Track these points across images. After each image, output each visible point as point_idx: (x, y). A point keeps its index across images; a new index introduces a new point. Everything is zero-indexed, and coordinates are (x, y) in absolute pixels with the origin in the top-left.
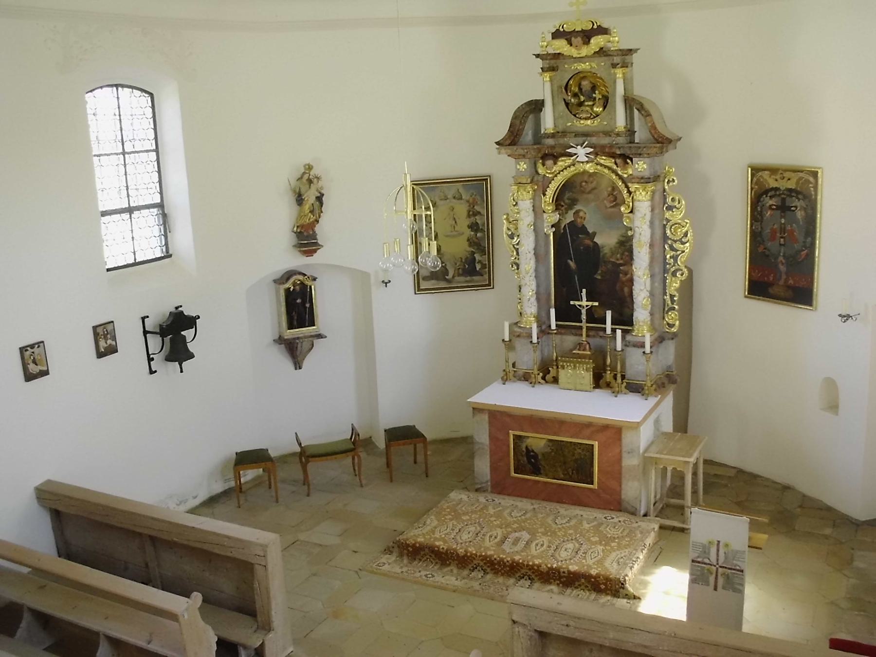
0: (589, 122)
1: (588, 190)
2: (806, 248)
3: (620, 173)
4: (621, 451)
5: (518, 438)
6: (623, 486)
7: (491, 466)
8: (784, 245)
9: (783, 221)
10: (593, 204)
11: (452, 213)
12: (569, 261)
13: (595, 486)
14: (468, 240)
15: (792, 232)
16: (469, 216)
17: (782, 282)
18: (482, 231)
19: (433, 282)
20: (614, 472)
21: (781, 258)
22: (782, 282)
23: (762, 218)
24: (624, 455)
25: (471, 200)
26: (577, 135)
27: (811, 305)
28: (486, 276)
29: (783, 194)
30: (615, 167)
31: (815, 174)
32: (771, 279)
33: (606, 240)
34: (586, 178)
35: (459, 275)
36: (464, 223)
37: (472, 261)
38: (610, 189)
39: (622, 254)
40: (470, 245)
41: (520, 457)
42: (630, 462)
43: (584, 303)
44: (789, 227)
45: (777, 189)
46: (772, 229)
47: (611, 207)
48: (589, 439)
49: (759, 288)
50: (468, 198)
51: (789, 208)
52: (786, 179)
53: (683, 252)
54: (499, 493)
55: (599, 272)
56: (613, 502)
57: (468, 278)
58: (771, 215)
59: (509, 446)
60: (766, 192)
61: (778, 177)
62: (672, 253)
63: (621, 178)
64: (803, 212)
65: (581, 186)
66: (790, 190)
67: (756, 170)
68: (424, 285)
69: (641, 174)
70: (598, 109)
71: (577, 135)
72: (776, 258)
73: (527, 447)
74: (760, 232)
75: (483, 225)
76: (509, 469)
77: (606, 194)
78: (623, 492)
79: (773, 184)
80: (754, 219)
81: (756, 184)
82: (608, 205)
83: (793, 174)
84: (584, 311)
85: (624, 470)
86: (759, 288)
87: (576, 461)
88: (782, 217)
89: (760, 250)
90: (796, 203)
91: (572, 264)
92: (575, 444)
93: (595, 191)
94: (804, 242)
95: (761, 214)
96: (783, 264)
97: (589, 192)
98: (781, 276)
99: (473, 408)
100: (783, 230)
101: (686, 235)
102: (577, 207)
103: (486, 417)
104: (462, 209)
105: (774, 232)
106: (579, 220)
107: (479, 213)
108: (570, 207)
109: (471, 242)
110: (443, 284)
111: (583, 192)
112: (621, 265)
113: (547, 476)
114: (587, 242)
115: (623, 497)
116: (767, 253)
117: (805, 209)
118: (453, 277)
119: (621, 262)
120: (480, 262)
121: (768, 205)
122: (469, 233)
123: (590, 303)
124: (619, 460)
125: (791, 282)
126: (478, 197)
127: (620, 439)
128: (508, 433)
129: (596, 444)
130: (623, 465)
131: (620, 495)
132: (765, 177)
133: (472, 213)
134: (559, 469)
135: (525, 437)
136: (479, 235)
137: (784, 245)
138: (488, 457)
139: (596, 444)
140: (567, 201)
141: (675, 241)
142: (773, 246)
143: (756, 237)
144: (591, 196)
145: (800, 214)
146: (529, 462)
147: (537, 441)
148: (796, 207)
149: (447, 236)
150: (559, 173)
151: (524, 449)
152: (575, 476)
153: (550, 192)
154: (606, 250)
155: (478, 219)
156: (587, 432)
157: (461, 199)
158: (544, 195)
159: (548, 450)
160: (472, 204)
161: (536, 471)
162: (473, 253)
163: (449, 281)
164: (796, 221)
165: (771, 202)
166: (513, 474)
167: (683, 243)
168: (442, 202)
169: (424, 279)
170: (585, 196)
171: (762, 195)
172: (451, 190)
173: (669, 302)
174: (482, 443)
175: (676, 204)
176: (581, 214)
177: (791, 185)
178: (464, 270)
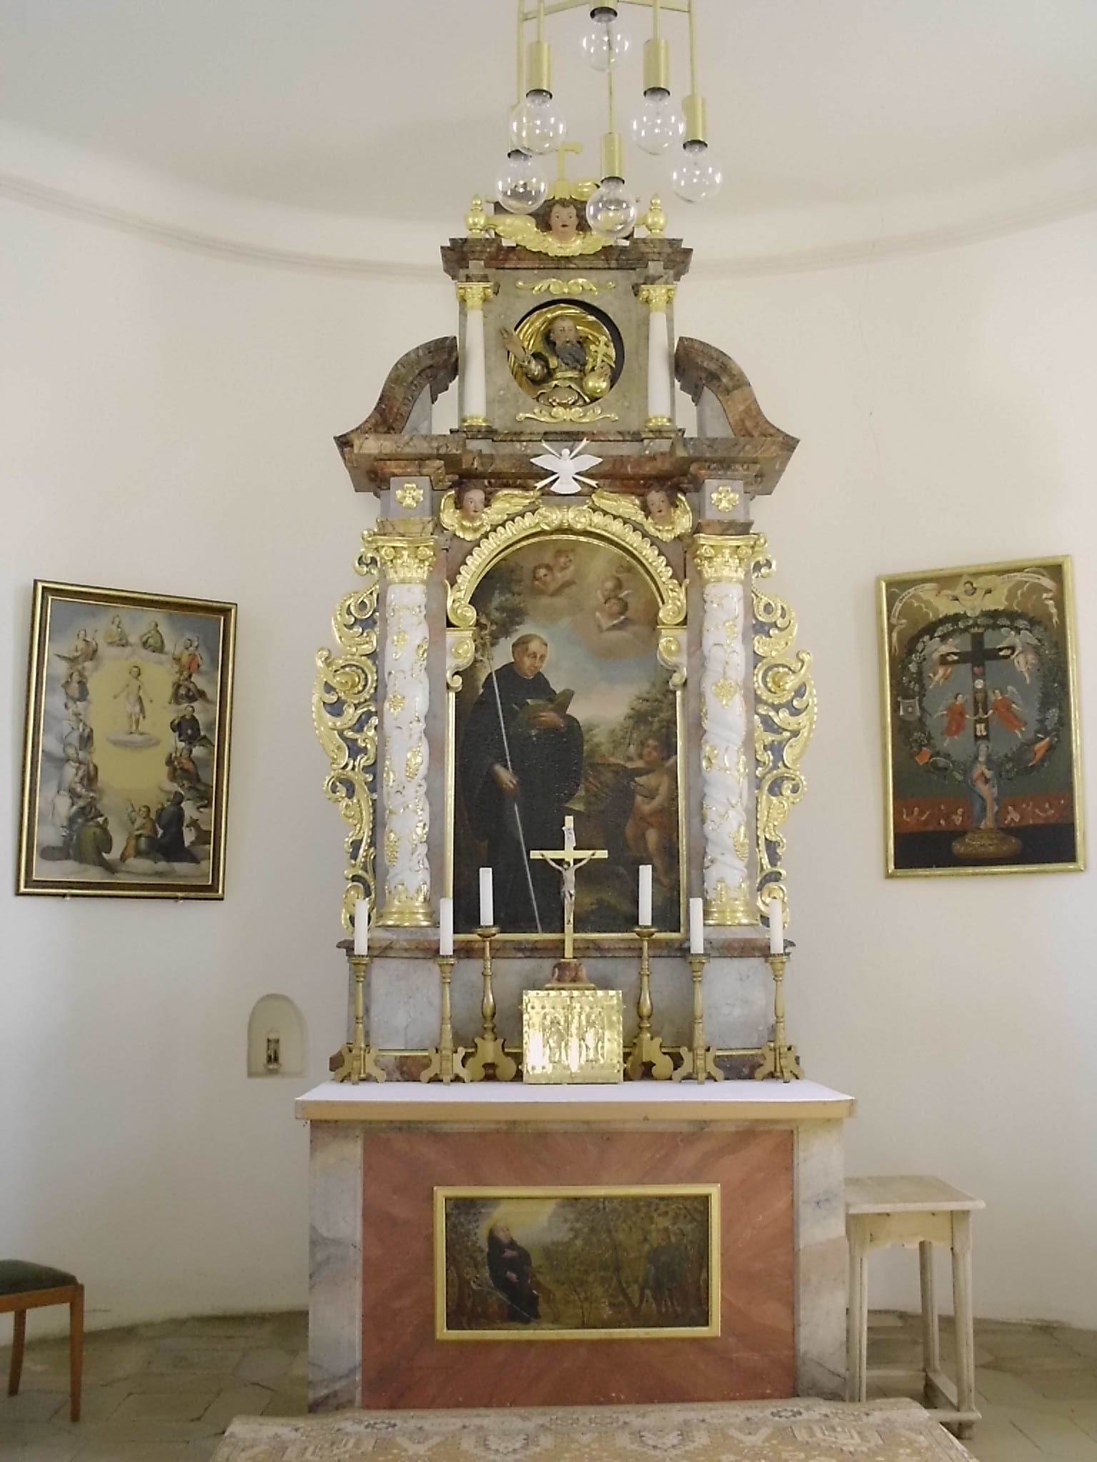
0: (577, 410)
1: (553, 587)
2: (1047, 734)
3: (652, 530)
4: (792, 1204)
5: (462, 1209)
6: (803, 1314)
7: (365, 1317)
8: (986, 738)
9: (979, 684)
10: (565, 622)
11: (135, 684)
12: (499, 768)
13: (714, 1329)
14: (169, 762)
15: (1006, 704)
16: (176, 698)
17: (987, 823)
18: (206, 742)
19: (70, 865)
20: (776, 1271)
21: (981, 768)
22: (987, 823)
23: (923, 687)
24: (806, 1212)
25: (185, 659)
26: (547, 436)
27: (1072, 858)
28: (208, 865)
29: (976, 625)
30: (640, 517)
31: (1056, 571)
32: (958, 820)
33: (601, 709)
34: (548, 558)
35: (139, 854)
36: (162, 715)
37: (172, 819)
38: (610, 585)
39: (642, 744)
40: (173, 777)
41: (469, 1273)
42: (820, 1231)
43: (569, 853)
44: (995, 696)
45: (956, 618)
46: (950, 709)
47: (614, 627)
48: (694, 1179)
49: (924, 845)
50: (177, 653)
51: (994, 654)
52: (980, 593)
53: (795, 734)
54: (393, 1407)
55: (581, 793)
56: (773, 1372)
57: (162, 865)
58: (946, 678)
59: (430, 1239)
60: (930, 629)
61: (959, 591)
62: (769, 738)
63: (654, 542)
64: (1031, 657)
65: (535, 578)
66: (994, 614)
67: (897, 587)
68: (43, 870)
69: (726, 518)
70: (597, 383)
71: (547, 436)
72: (967, 771)
73: (492, 1238)
74: (921, 720)
75: (210, 727)
76: (431, 1317)
77: (600, 597)
78: (803, 1332)
79: (946, 607)
80: (900, 691)
81: (902, 614)
82: (606, 623)
83: (998, 579)
84: (570, 876)
85: (803, 1260)
86: (924, 845)
87: (653, 1256)
88: (975, 677)
89: (922, 760)
90: (1011, 638)
91: (506, 776)
92: (650, 1201)
93: (574, 588)
94: (1041, 721)
95: (920, 677)
96: (987, 781)
97: (553, 594)
98: (984, 809)
99: (316, 1125)
100: (981, 703)
101: (800, 692)
102: (522, 630)
103: (354, 1150)
104: (160, 677)
105: (956, 715)
106: (527, 662)
107: (202, 694)
108: (504, 629)
109: (176, 769)
110: (94, 874)
111: (541, 592)
112: (639, 772)
113: (557, 1321)
114: (549, 716)
115: (803, 1347)
116: (941, 761)
117: (1036, 650)
118: (123, 858)
119: (639, 764)
120: (194, 823)
121: (936, 656)
122: (172, 742)
123: (586, 854)
124: (789, 1233)
125: (1014, 816)
126: (203, 655)
127: (789, 1167)
128: (430, 1198)
129: (443, 1333)
130: (802, 1243)
131: (793, 1347)
132: (925, 596)
133: (186, 693)
134: (598, 1291)
135: (497, 1200)
136: (198, 751)
137: (986, 738)
138: (358, 1287)
139: (714, 1191)
140: (496, 615)
141: (777, 709)
142: (954, 745)
143: (908, 736)
144: (559, 601)
145: (1023, 663)
146: (501, 1282)
147: (528, 1212)
148: (1013, 649)
149: (116, 743)
150: (503, 524)
151: (483, 1243)
152: (651, 1307)
153: (469, 576)
154: (600, 737)
155: (201, 712)
156: (689, 1157)
157: (160, 649)
158: (453, 583)
159: (562, 1234)
160: (188, 668)
161: (523, 1307)
162: (178, 800)
163: (110, 868)
164: (1016, 678)
165: (944, 649)
166: (443, 1333)
167: (796, 712)
168: (115, 651)
169: (49, 853)
170: (545, 601)
171: (916, 639)
172: (140, 623)
173: (765, 861)
174: (336, 1242)
175: (776, 617)
176: (534, 646)
177: (997, 602)
178: (152, 839)
